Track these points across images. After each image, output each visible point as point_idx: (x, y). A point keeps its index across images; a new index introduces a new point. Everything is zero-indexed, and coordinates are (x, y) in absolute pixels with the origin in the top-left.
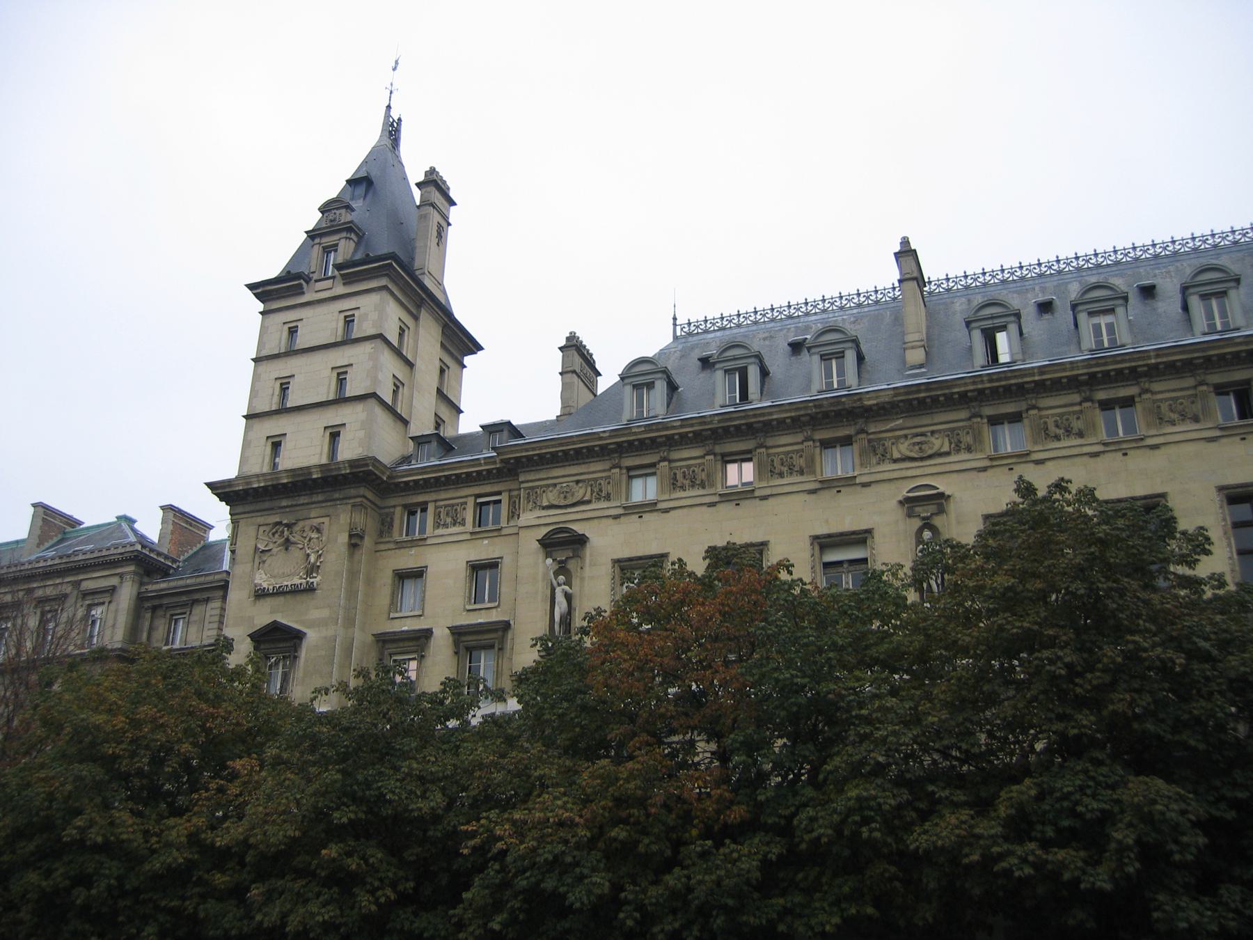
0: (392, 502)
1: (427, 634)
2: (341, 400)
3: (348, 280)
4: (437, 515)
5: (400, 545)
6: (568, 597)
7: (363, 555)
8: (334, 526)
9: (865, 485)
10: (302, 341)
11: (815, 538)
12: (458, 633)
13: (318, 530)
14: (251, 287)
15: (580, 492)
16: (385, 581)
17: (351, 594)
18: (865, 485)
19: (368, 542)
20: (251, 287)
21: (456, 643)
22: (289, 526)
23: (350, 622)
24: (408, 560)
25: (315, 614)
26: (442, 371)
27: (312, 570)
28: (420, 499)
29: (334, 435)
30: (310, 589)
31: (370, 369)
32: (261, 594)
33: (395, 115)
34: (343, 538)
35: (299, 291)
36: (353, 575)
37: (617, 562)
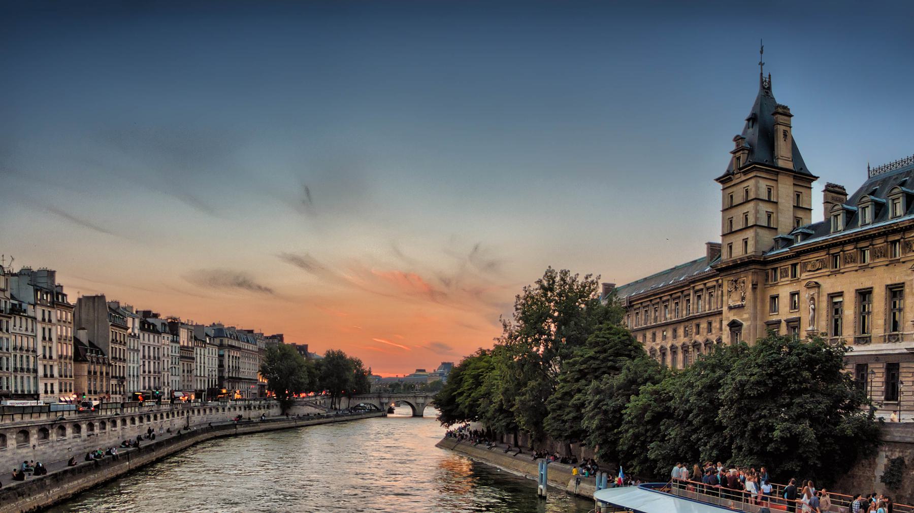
0: (769, 267)
1: (779, 322)
2: (747, 228)
3: (745, 173)
4: (781, 273)
5: (772, 286)
6: (814, 310)
7: (758, 291)
8: (748, 279)
9: (904, 262)
10: (736, 202)
11: (887, 286)
12: (788, 322)
13: (744, 283)
14: (717, 180)
15: (818, 265)
16: (768, 300)
17: (755, 307)
18: (904, 262)
19: (759, 286)
20: (717, 180)
21: (787, 325)
22: (736, 281)
23: (755, 318)
24: (773, 292)
25: (746, 316)
26: (798, 196)
27: (743, 299)
28: (776, 266)
29: (746, 242)
30: (742, 307)
31: (755, 212)
32: (730, 308)
33: (766, 75)
34: (750, 286)
35: (730, 180)
36: (755, 299)
37: (829, 294)
